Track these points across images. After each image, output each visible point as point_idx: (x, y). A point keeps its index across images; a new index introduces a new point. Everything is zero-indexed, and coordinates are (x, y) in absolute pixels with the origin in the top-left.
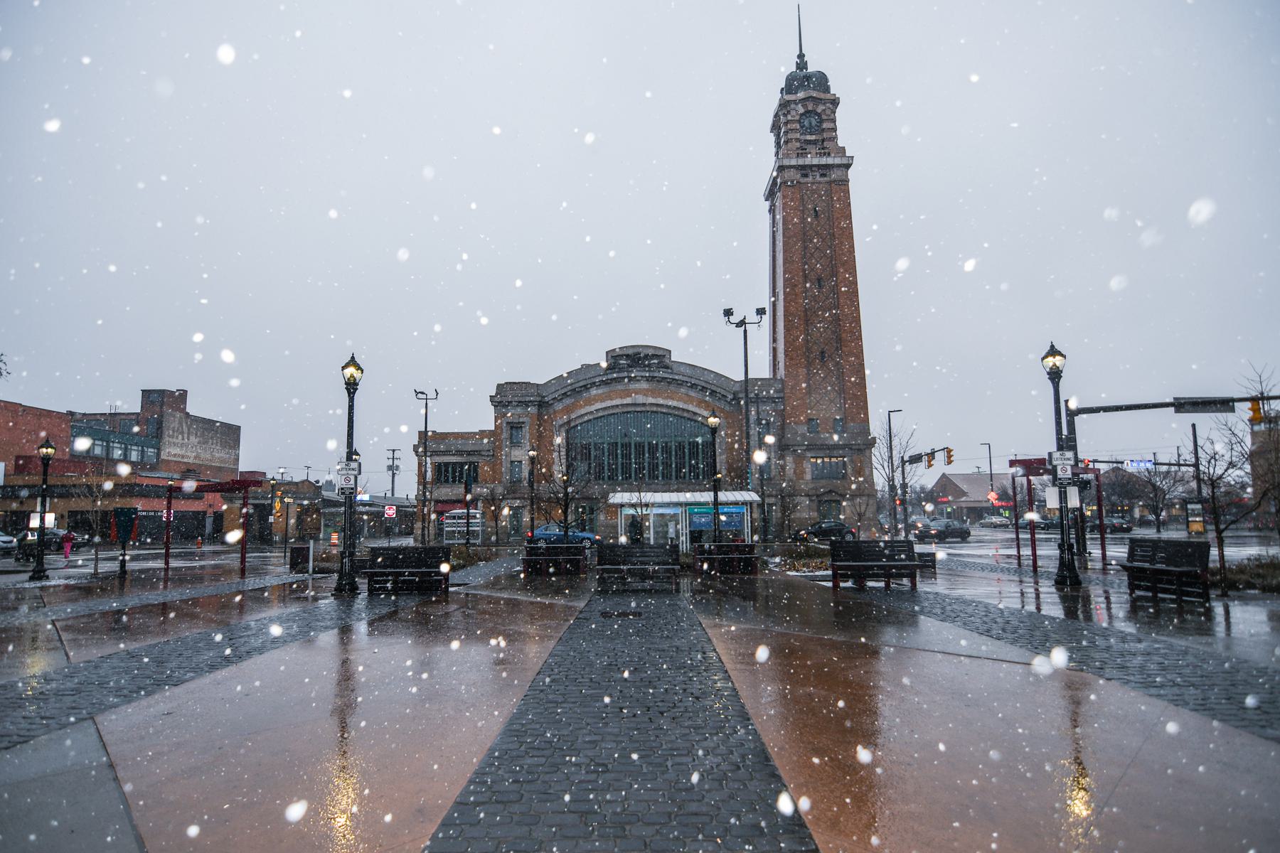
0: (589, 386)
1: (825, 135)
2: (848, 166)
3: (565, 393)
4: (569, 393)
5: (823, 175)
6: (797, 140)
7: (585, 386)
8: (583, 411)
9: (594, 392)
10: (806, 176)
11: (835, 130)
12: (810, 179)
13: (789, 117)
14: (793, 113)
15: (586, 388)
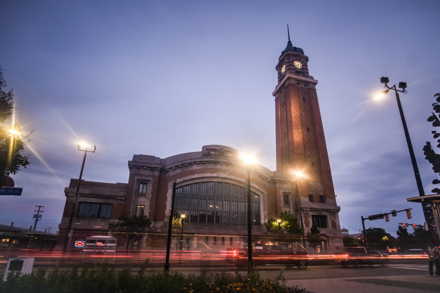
0: (192, 164)
1: (305, 71)
2: (316, 84)
3: (177, 166)
4: (180, 166)
5: (305, 85)
6: (294, 69)
7: (189, 163)
8: (187, 178)
9: (195, 167)
10: (298, 84)
11: (307, 69)
12: (300, 86)
13: (290, 60)
14: (291, 58)
15: (190, 164)
